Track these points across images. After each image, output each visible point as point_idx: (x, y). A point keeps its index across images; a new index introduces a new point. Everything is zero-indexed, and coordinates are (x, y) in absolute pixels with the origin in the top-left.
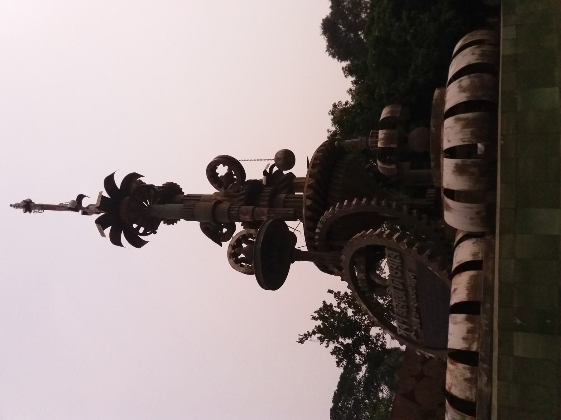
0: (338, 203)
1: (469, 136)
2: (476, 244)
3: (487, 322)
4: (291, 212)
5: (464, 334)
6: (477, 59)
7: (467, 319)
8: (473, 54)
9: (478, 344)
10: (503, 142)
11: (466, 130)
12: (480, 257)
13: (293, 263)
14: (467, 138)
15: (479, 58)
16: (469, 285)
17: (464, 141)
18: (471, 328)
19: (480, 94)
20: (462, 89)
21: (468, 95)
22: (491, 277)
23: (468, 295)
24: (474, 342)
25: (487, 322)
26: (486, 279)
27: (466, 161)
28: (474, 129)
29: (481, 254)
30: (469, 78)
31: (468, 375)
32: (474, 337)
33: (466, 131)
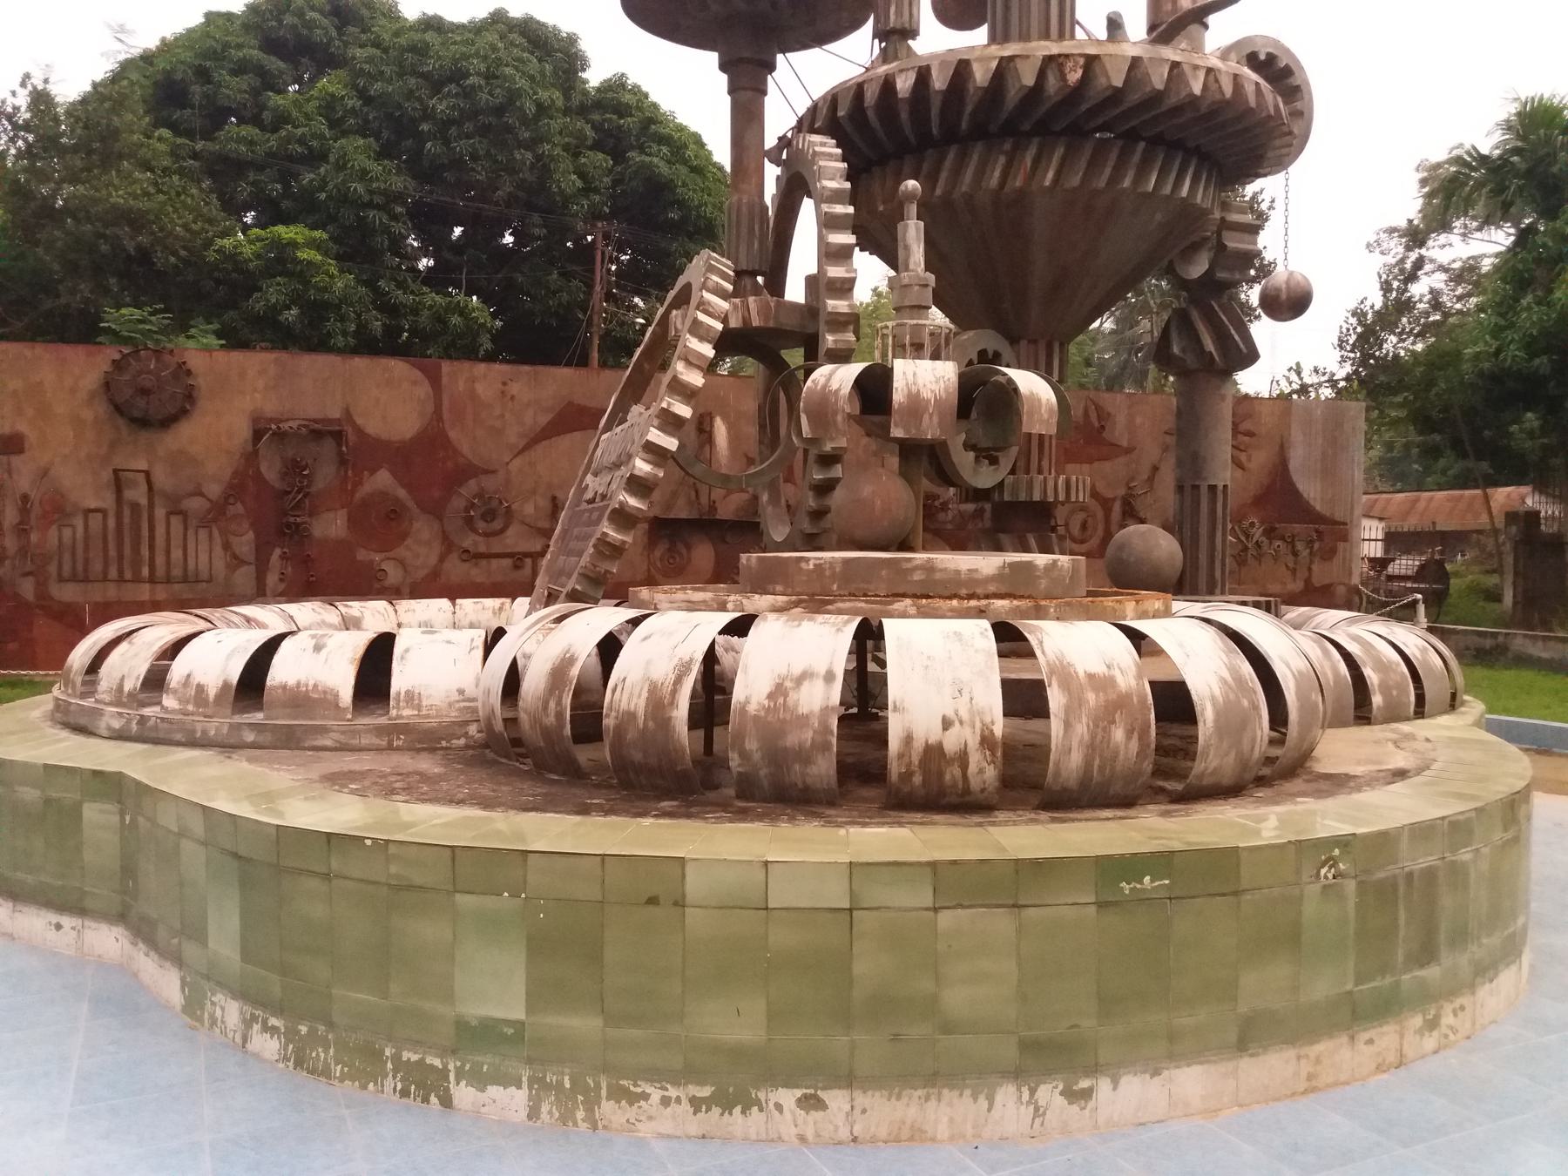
0: (851, 210)
1: (624, 706)
2: (456, 697)
3: (212, 733)
4: (892, 17)
5: (198, 678)
6: (908, 739)
7: (226, 685)
8: (947, 724)
9: (173, 711)
10: (369, 842)
11: (645, 694)
12: (400, 712)
13: (724, 67)
14: (620, 701)
15: (918, 745)
16: (310, 688)
17: (614, 691)
18: (207, 695)
19: (752, 745)
20: (788, 684)
21: (752, 708)
22: (328, 743)
23: (284, 687)
24: (180, 701)
25: (212, 733)
26: (323, 730)
27: (570, 690)
28: (641, 721)
29: (416, 713)
30: (826, 710)
31: (128, 687)
32: (188, 702)
33: (640, 695)
